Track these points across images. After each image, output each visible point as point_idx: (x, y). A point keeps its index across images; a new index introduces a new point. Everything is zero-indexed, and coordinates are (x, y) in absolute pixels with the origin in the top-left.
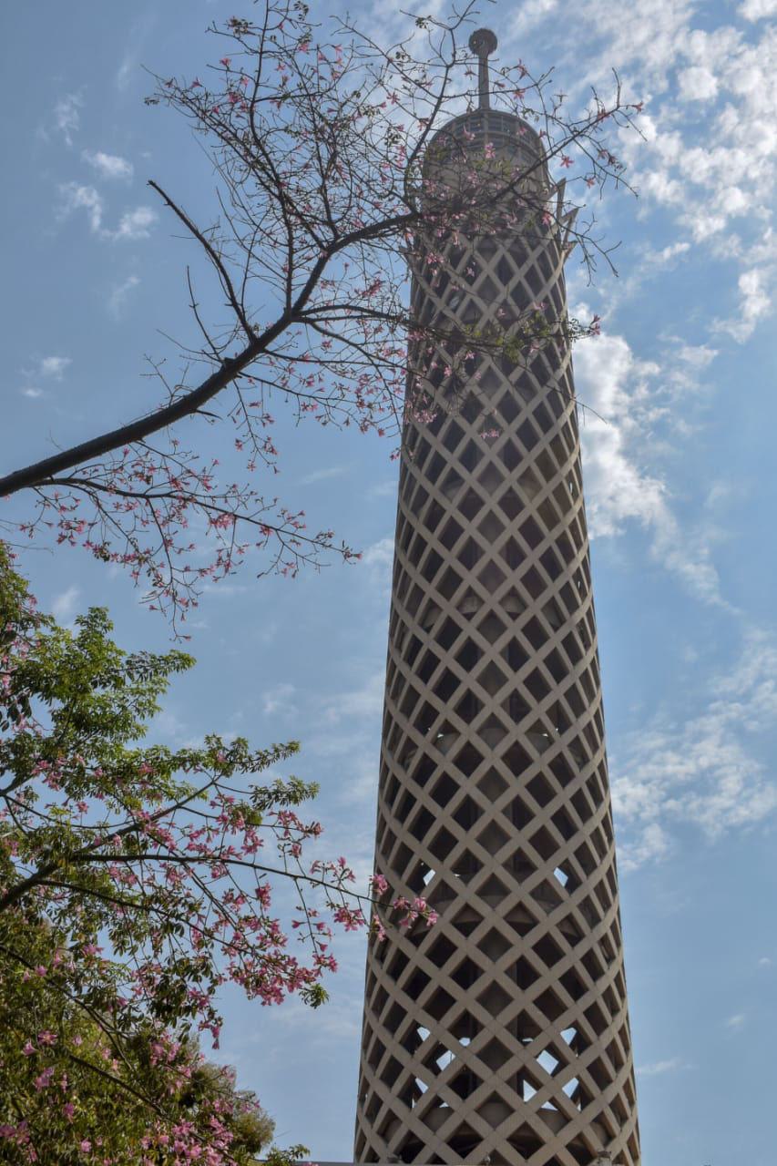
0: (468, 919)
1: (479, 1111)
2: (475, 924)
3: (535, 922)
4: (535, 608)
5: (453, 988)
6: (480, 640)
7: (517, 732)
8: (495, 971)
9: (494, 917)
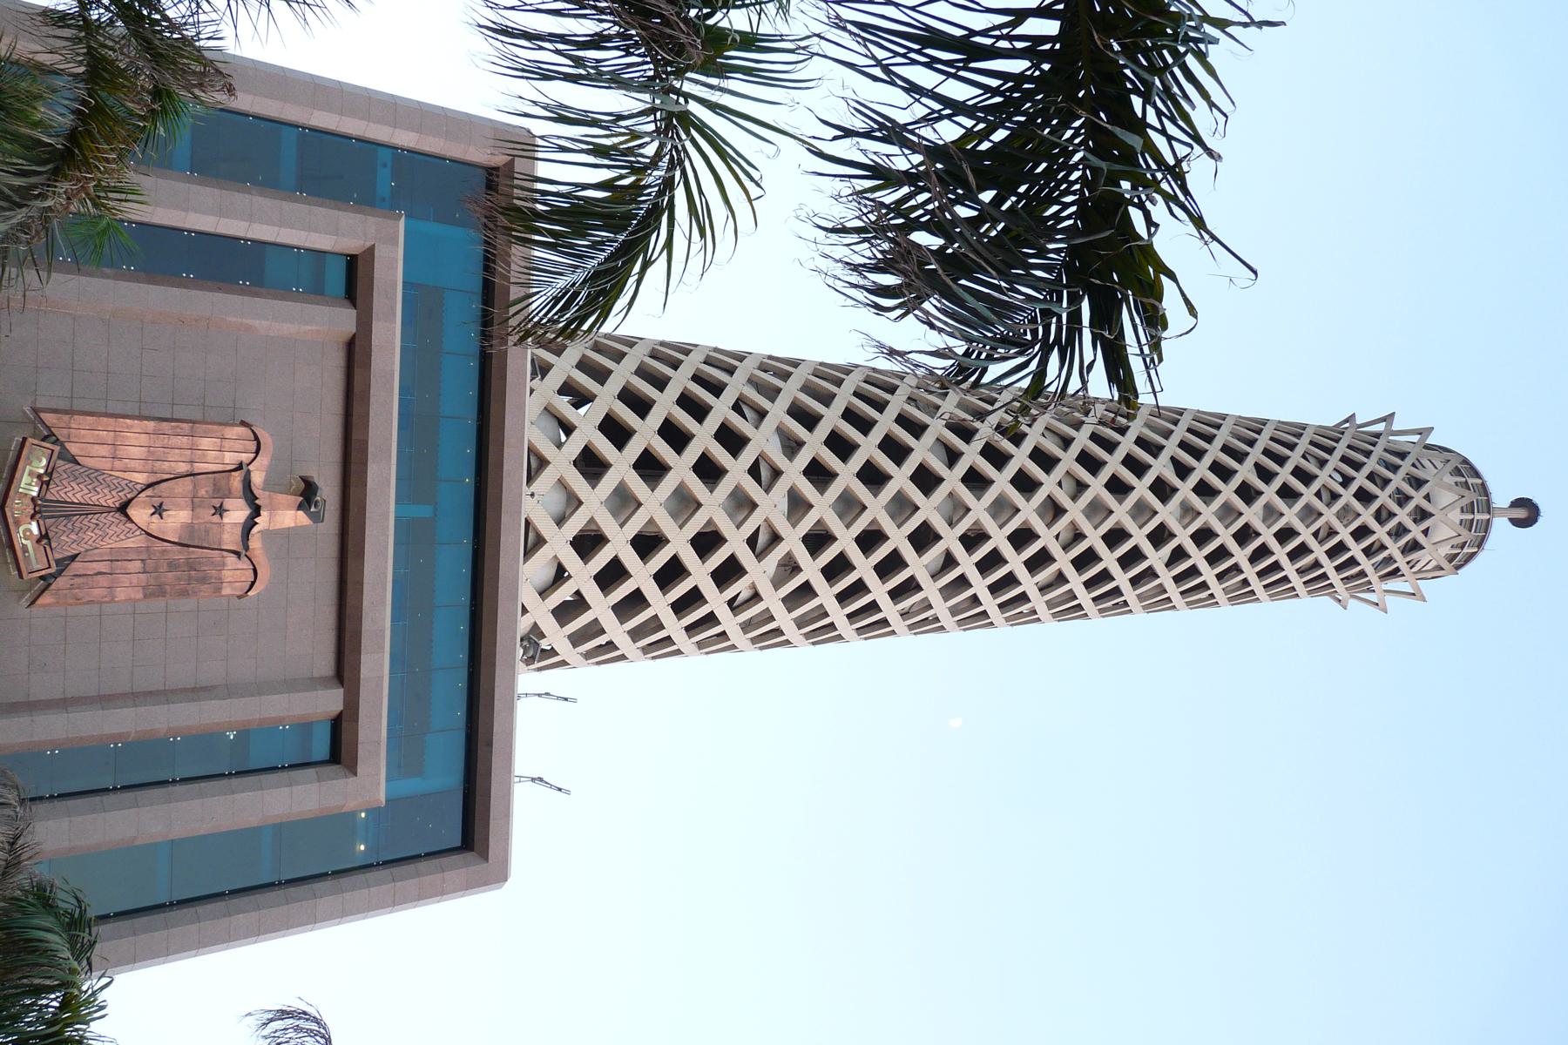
0: (765, 473)
1: (562, 483)
3: (760, 556)
4: (1063, 561)
5: (692, 453)
6: (1040, 496)
7: (950, 540)
8: (713, 506)
9: (771, 506)
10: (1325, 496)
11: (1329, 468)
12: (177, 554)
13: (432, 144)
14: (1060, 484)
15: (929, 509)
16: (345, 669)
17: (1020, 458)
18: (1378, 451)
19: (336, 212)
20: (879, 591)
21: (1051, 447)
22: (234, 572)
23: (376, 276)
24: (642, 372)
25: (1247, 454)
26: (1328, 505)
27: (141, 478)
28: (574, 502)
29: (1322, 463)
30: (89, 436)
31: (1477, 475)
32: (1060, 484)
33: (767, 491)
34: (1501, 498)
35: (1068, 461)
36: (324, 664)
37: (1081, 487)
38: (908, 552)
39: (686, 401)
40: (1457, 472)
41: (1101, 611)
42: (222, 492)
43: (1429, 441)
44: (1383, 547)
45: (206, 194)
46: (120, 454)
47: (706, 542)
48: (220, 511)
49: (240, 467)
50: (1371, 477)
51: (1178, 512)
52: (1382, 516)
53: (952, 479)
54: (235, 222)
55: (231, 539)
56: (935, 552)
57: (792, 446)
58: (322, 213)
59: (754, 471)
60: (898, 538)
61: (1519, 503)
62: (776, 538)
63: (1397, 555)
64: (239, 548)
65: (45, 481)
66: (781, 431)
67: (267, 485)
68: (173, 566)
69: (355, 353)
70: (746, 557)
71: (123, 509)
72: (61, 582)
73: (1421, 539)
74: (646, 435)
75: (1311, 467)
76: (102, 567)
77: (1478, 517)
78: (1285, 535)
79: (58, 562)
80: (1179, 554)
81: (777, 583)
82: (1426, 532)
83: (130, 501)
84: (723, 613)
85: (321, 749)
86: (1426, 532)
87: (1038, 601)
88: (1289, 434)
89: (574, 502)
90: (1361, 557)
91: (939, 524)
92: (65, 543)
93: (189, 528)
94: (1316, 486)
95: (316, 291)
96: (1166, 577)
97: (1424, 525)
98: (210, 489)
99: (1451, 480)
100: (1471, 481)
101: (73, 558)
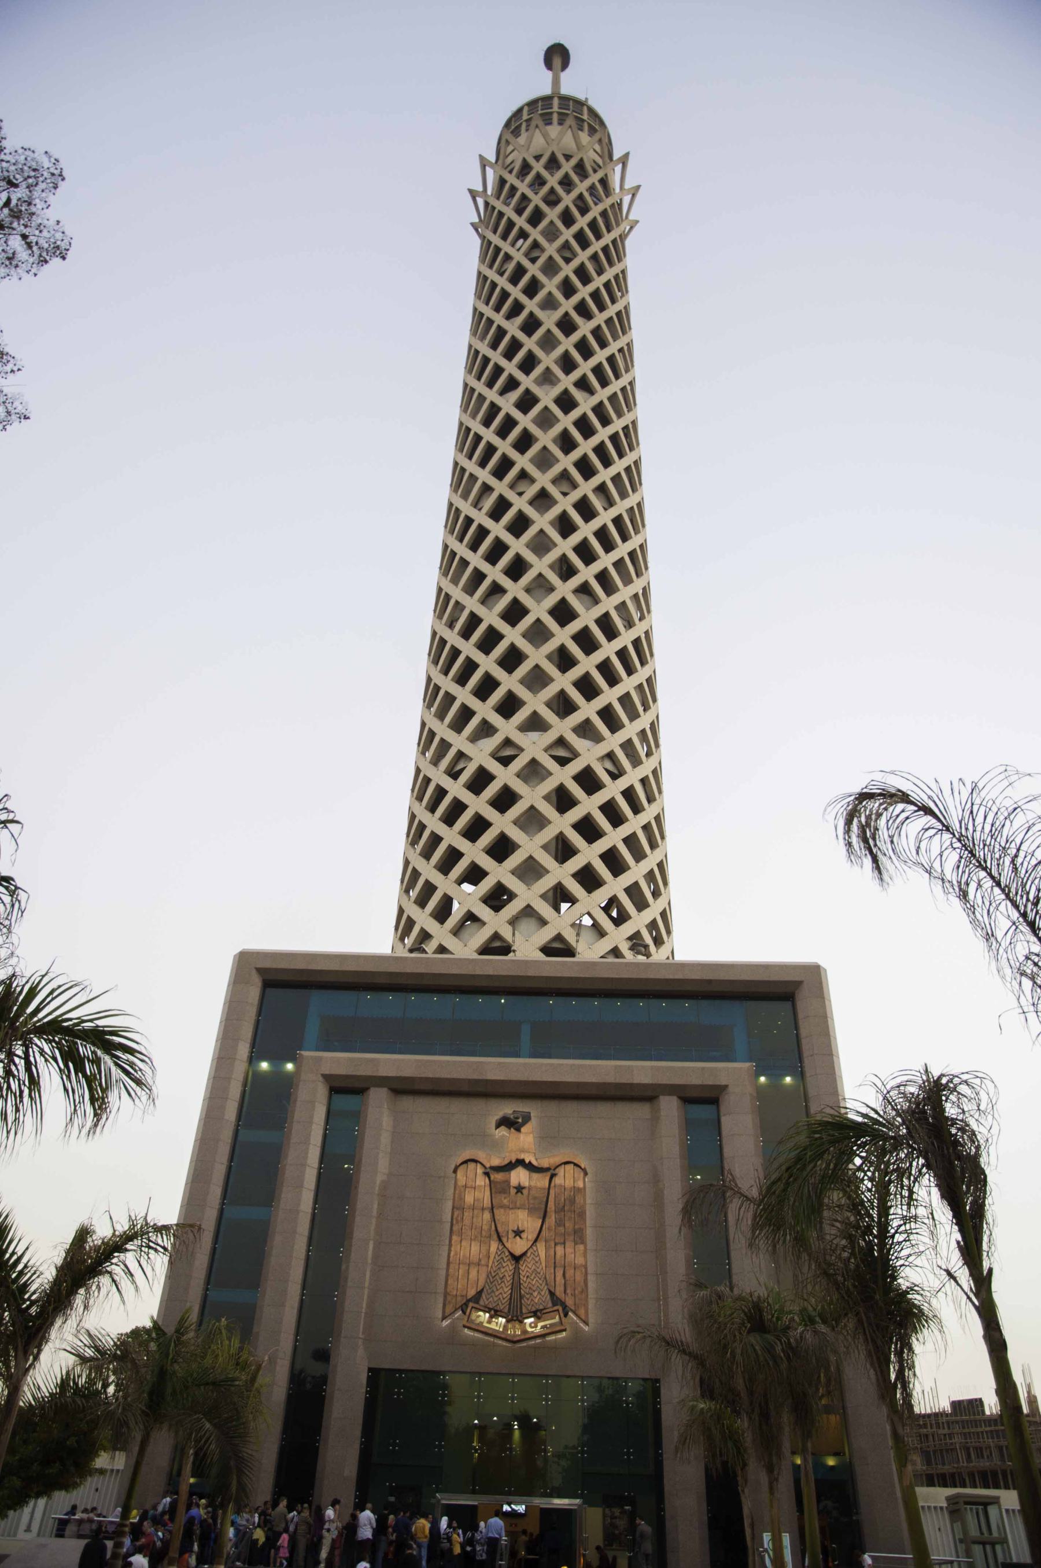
0: (508, 752)
1: (513, 922)
2: (513, 758)
3: (576, 755)
4: (586, 488)
5: (490, 814)
6: (530, 512)
9: (534, 746)
10: (534, 254)
11: (512, 251)
12: (551, 1219)
13: (247, 1031)
14: (520, 494)
15: (539, 610)
16: (644, 1095)
17: (498, 530)
18: (499, 205)
19: (298, 1104)
20: (608, 650)
21: (489, 503)
22: (566, 1178)
23: (344, 1073)
24: (427, 854)
25: (499, 327)
26: (543, 250)
27: (494, 1246)
28: (528, 911)
29: (508, 257)
30: (462, 1284)
31: (520, 111)
32: (520, 494)
33: (522, 750)
34: (541, 84)
35: (501, 487)
36: (641, 1111)
37: (523, 475)
38: (575, 626)
39: (449, 819)
40: (516, 133)
41: (631, 449)
43: (493, 160)
44: (581, 196)
45: (286, 1195)
46: (476, 1260)
47: (563, 801)
48: (519, 1189)
49: (487, 1174)
50: (519, 211)
51: (546, 387)
52: (552, 200)
53: (515, 590)
54: (307, 1176)
55: (541, 1181)
56: (574, 602)
57: (486, 729)
58: (299, 1113)
59: (506, 761)
60: (563, 636)
61: (548, 63)
62: (561, 742)
63: (587, 183)
64: (549, 1174)
65: (495, 1313)
66: (474, 738)
68: (560, 1223)
69: (403, 1088)
70: (576, 767)
71: (517, 1259)
73: (573, 162)
74: (474, 853)
75: (511, 267)
77: (556, 108)
78: (568, 289)
79: (554, 1305)
80: (582, 384)
81: (598, 738)
82: (568, 157)
83: (511, 1254)
84: (623, 783)
86: (568, 157)
87: (621, 507)
88: (485, 288)
89: (528, 911)
90: (589, 217)
91: (551, 600)
92: (539, 1298)
93: (531, 1211)
94: (526, 263)
95: (357, 1116)
96: (603, 395)
97: (561, 159)
98: (503, 1196)
99: (522, 140)
100: (525, 117)
101: (552, 1294)
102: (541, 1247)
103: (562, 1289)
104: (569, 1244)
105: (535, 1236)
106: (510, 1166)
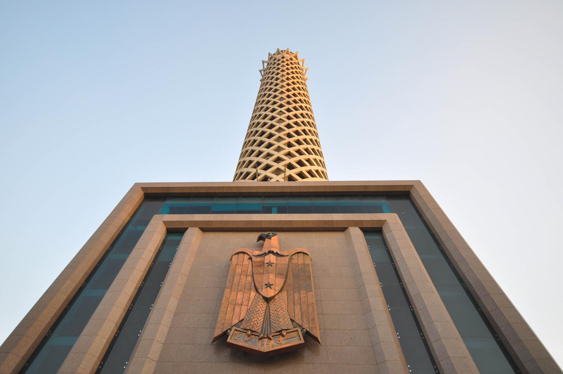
12: (290, 280)
16: (341, 228)
27: (253, 294)
42: (262, 264)
46: (240, 302)
48: (270, 264)
49: (250, 258)
64: (287, 259)
67: (261, 250)
71: (267, 300)
72: (306, 326)
76: (297, 308)
83: (264, 297)
85: (375, 237)
93: (278, 274)
98: (260, 268)
102: (284, 293)
103: (300, 317)
104: (302, 292)
105: (280, 288)
106: (265, 254)
